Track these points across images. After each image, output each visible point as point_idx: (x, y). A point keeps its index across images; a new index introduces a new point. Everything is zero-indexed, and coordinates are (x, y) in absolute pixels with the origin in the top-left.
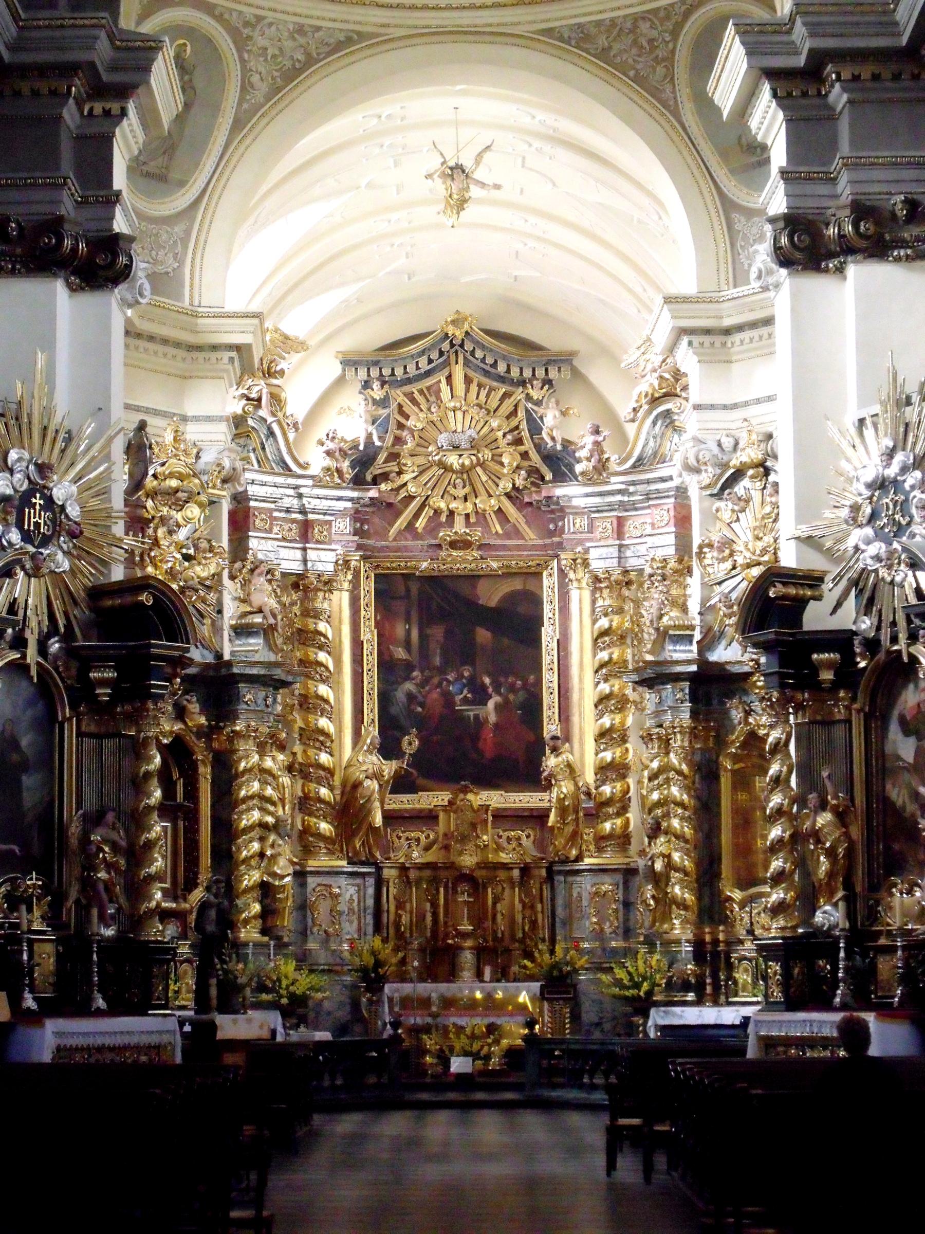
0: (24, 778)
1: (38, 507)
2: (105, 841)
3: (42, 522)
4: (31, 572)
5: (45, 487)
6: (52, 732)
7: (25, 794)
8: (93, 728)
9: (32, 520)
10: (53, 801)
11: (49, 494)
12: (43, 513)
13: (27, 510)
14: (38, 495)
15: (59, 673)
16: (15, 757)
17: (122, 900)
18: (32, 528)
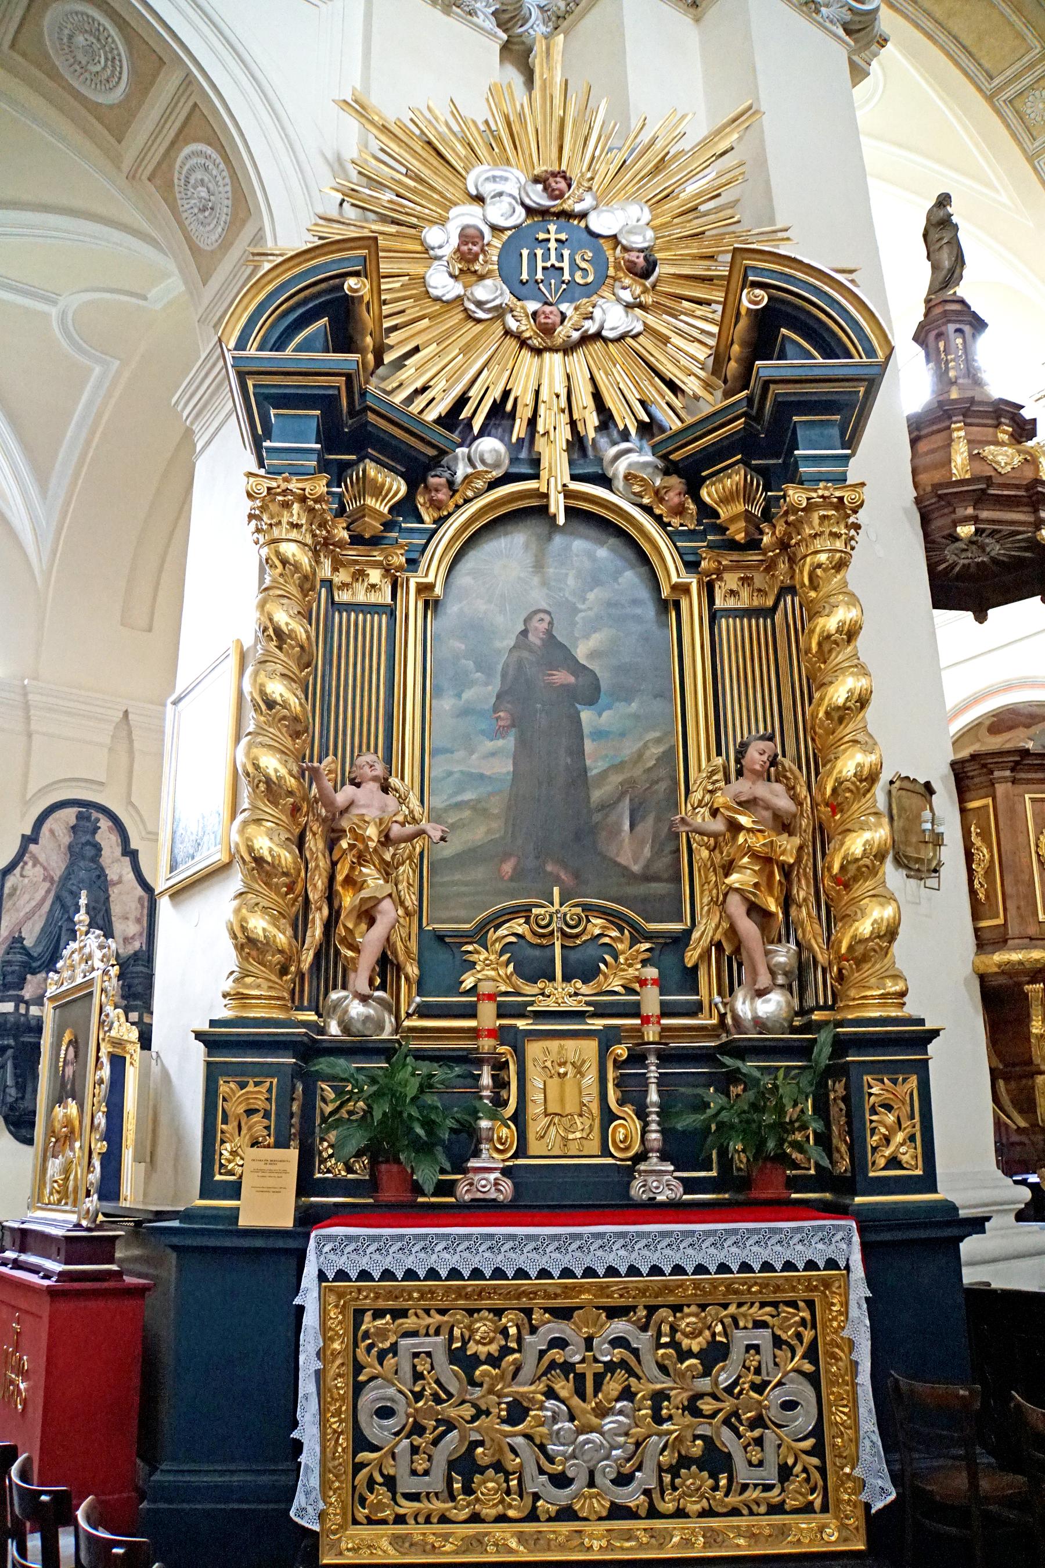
0: (586, 715)
1: (553, 245)
2: (749, 804)
3: (566, 265)
4: (536, 342)
5: (566, 215)
6: (666, 625)
7: (589, 746)
8: (745, 600)
9: (540, 264)
10: (671, 751)
11: (583, 224)
12: (566, 253)
13: (525, 252)
14: (552, 228)
15: (647, 509)
16: (563, 677)
17: (812, 933)
18: (540, 276)
